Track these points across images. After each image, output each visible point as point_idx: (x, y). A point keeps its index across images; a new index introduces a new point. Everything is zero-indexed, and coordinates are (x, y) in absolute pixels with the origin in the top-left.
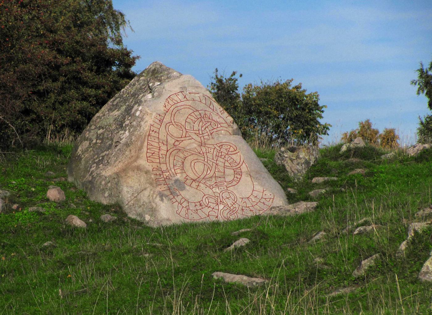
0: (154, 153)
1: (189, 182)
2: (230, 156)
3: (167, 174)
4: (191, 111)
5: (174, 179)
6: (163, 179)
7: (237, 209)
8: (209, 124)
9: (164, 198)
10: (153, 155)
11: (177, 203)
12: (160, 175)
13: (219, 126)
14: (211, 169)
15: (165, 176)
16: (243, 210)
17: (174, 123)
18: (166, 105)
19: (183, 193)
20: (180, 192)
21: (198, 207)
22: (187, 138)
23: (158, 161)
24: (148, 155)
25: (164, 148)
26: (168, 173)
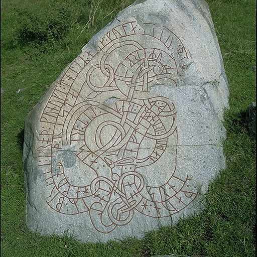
1: (85, 154)
2: (163, 119)
5: (66, 148)
8: (152, 68)
12: (48, 141)
14: (123, 136)
16: (145, 205)
18: (105, 39)
19: (68, 171)
21: (81, 195)
25: (71, 100)
26: (60, 139)
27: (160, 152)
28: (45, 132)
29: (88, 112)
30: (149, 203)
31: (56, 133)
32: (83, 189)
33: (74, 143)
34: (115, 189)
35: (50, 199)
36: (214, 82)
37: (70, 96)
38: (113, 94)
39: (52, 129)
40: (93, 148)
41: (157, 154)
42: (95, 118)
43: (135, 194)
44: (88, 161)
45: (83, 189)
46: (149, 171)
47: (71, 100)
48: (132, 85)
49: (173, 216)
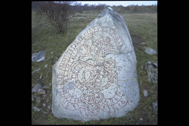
3: (66, 78)
4: (98, 38)
6: (62, 81)
7: (100, 106)
10: (64, 65)
11: (64, 98)
12: (62, 78)
15: (64, 79)
18: (86, 33)
19: (71, 92)
21: (77, 102)
22: (88, 55)
23: (64, 69)
25: (72, 60)
26: (67, 78)
28: (61, 74)
29: (79, 66)
30: (106, 106)
31: (65, 75)
32: (77, 99)
33: (73, 80)
34: (91, 99)
35: (63, 103)
36: (131, 52)
39: (64, 73)
40: (81, 81)
41: (109, 84)
42: (82, 68)
43: (100, 102)
44: (79, 87)
45: (77, 99)
46: (105, 92)
47: (72, 60)
48: (98, 54)
49: (116, 112)
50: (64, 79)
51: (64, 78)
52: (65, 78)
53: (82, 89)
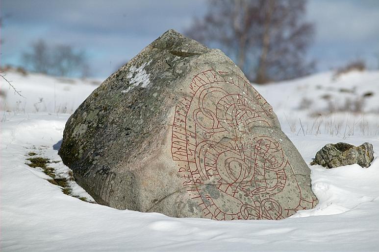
0: (180, 148)
1: (223, 187)
5: (207, 182)
9: (194, 208)
13: (256, 115)
15: (195, 179)
17: (202, 110)
18: (193, 86)
20: (215, 201)
22: (220, 130)
24: (174, 150)
25: (192, 141)
26: (199, 175)
27: (283, 181)
33: (212, 179)
37: (190, 138)
38: (226, 134)
40: (231, 181)
47: (192, 141)
50: (195, 179)
51: (194, 177)
52: (194, 176)
53: (237, 195)
